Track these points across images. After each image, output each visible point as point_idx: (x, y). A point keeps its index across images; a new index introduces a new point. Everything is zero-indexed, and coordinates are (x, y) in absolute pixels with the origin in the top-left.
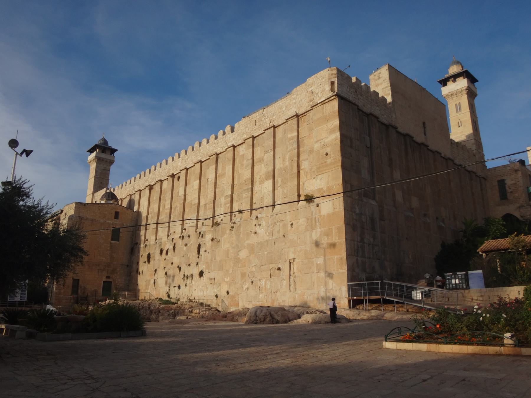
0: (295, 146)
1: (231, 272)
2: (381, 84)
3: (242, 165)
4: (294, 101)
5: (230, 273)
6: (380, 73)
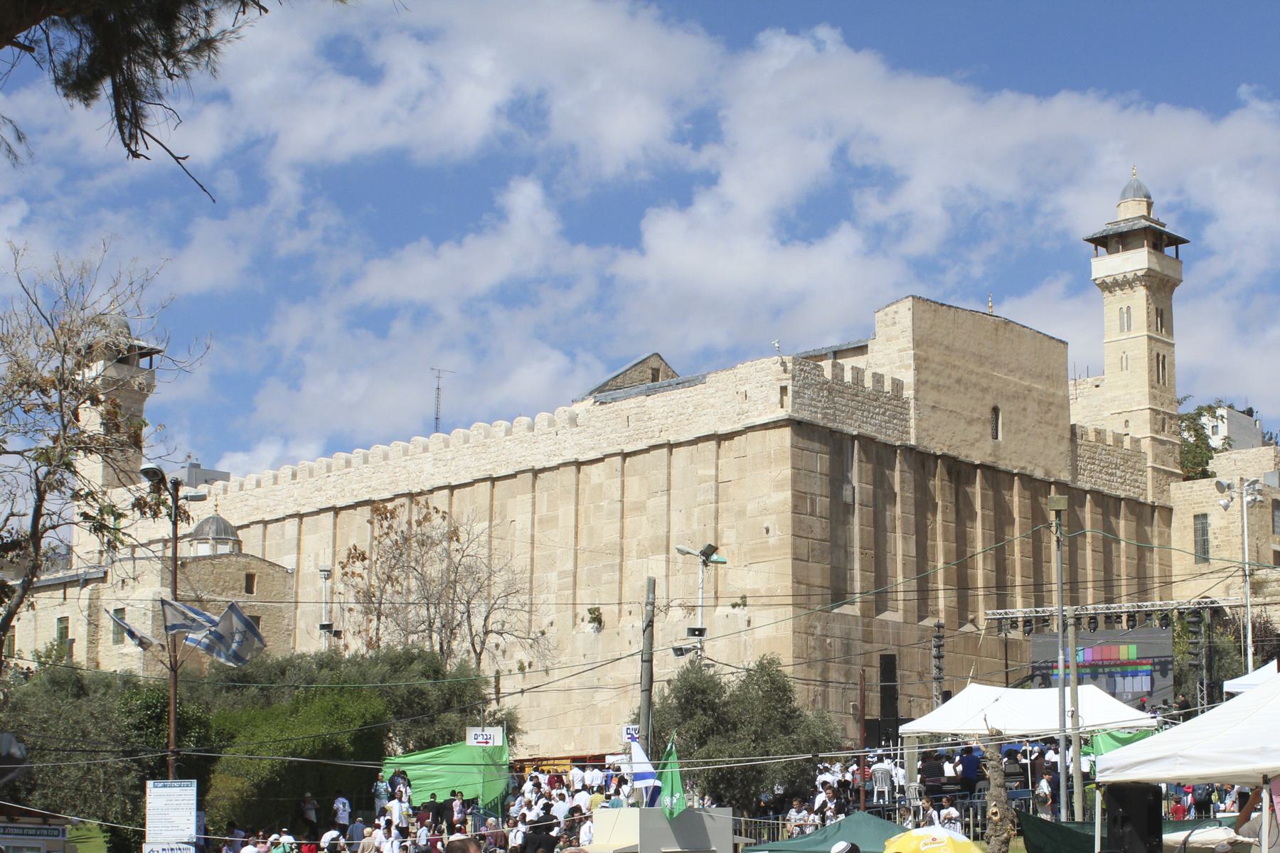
0: (713, 497)
1: (576, 731)
2: (897, 338)
3: (599, 508)
4: (711, 401)
5: (575, 734)
6: (896, 312)
